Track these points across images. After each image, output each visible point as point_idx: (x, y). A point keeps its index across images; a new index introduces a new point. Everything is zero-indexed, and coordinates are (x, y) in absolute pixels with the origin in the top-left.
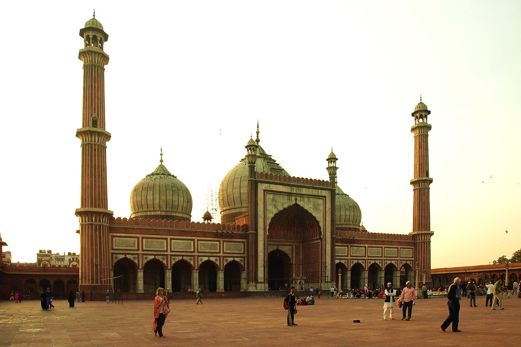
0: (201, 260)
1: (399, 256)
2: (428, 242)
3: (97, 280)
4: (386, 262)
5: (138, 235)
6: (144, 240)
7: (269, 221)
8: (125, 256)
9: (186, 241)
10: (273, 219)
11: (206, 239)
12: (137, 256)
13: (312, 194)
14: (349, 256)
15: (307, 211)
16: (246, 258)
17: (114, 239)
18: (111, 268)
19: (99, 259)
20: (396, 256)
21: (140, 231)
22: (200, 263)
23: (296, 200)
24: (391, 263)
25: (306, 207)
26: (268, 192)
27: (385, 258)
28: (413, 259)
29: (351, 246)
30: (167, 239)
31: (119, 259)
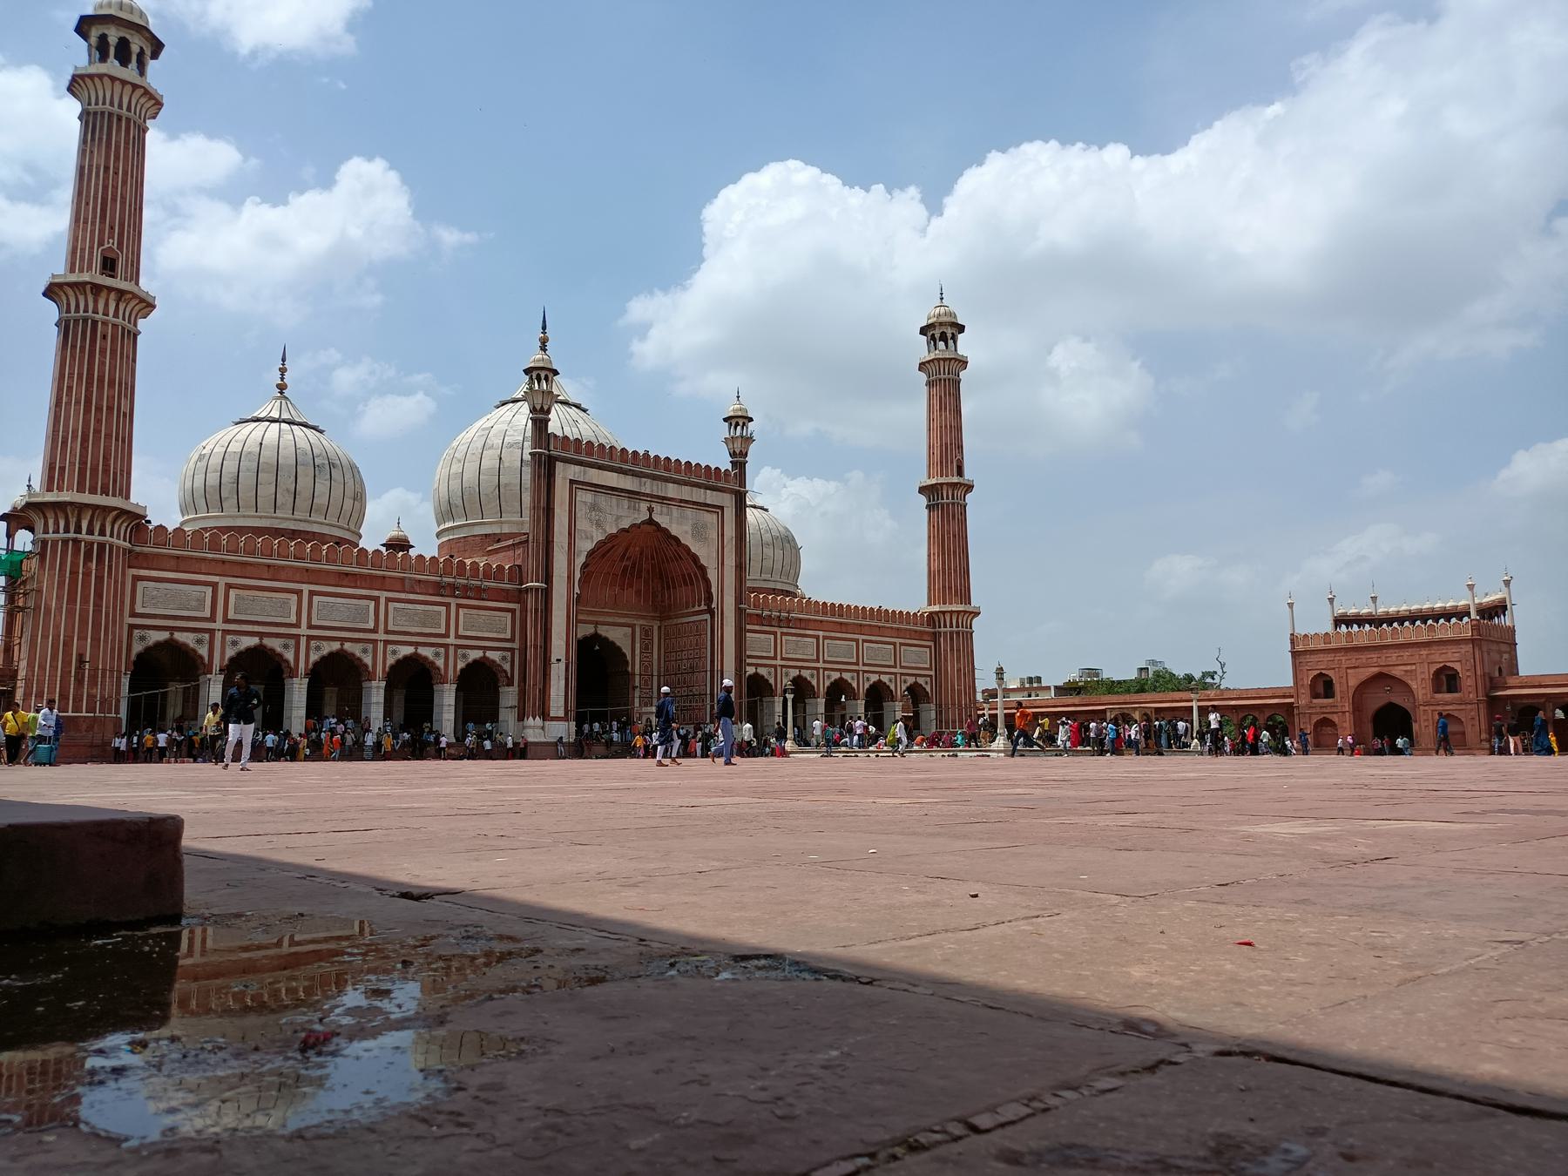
0: (394, 652)
1: (898, 666)
2: (967, 632)
3: (78, 699)
4: (868, 679)
6: (232, 593)
7: (580, 560)
8: (172, 634)
10: (591, 554)
11: (412, 597)
12: (207, 636)
14: (779, 657)
16: (517, 652)
17: (140, 585)
18: (123, 670)
19: (89, 640)
21: (223, 567)
22: (391, 661)
23: (650, 510)
24: (880, 681)
25: (675, 530)
26: (581, 487)
27: (866, 668)
29: (782, 634)
30: (299, 593)
31: (151, 643)
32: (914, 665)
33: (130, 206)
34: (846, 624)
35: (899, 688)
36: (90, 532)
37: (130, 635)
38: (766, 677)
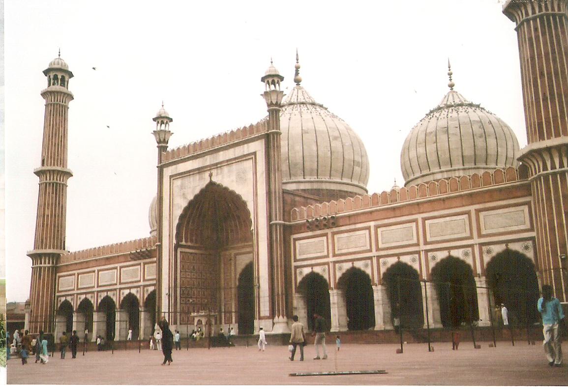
2: (554, 175)
4: (434, 258)
5: (74, 272)
7: (176, 222)
9: (111, 271)
10: (182, 217)
11: (128, 263)
13: (234, 157)
14: (331, 255)
15: (226, 189)
20: (464, 235)
23: (211, 175)
24: (450, 258)
26: (175, 178)
28: (534, 234)
29: (334, 234)
32: (502, 230)
33: (49, 136)
34: (399, 208)
35: (477, 262)
36: (35, 265)
37: (57, 299)
38: (321, 274)
